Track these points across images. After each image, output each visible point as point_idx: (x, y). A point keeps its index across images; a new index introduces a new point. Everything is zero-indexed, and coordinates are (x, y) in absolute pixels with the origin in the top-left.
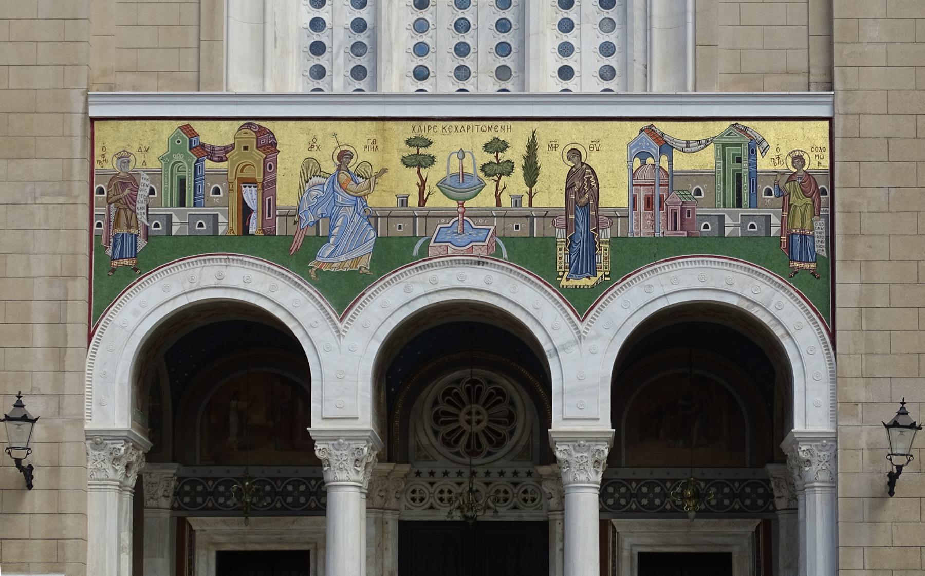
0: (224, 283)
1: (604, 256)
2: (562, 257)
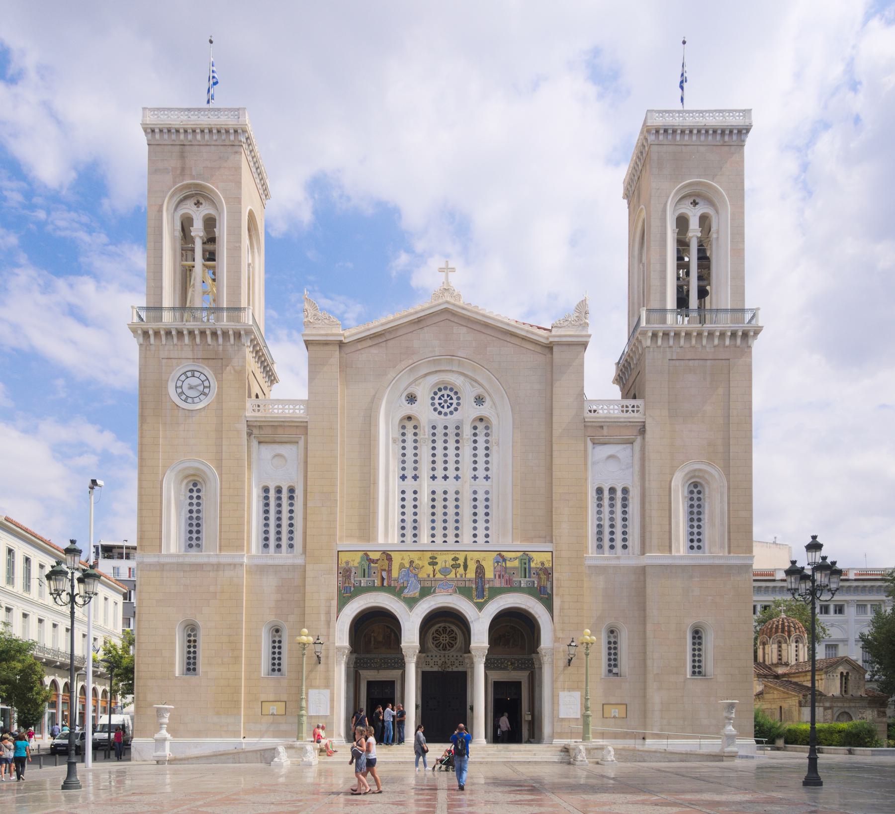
0: (377, 601)
1: (486, 593)
2: (474, 593)
